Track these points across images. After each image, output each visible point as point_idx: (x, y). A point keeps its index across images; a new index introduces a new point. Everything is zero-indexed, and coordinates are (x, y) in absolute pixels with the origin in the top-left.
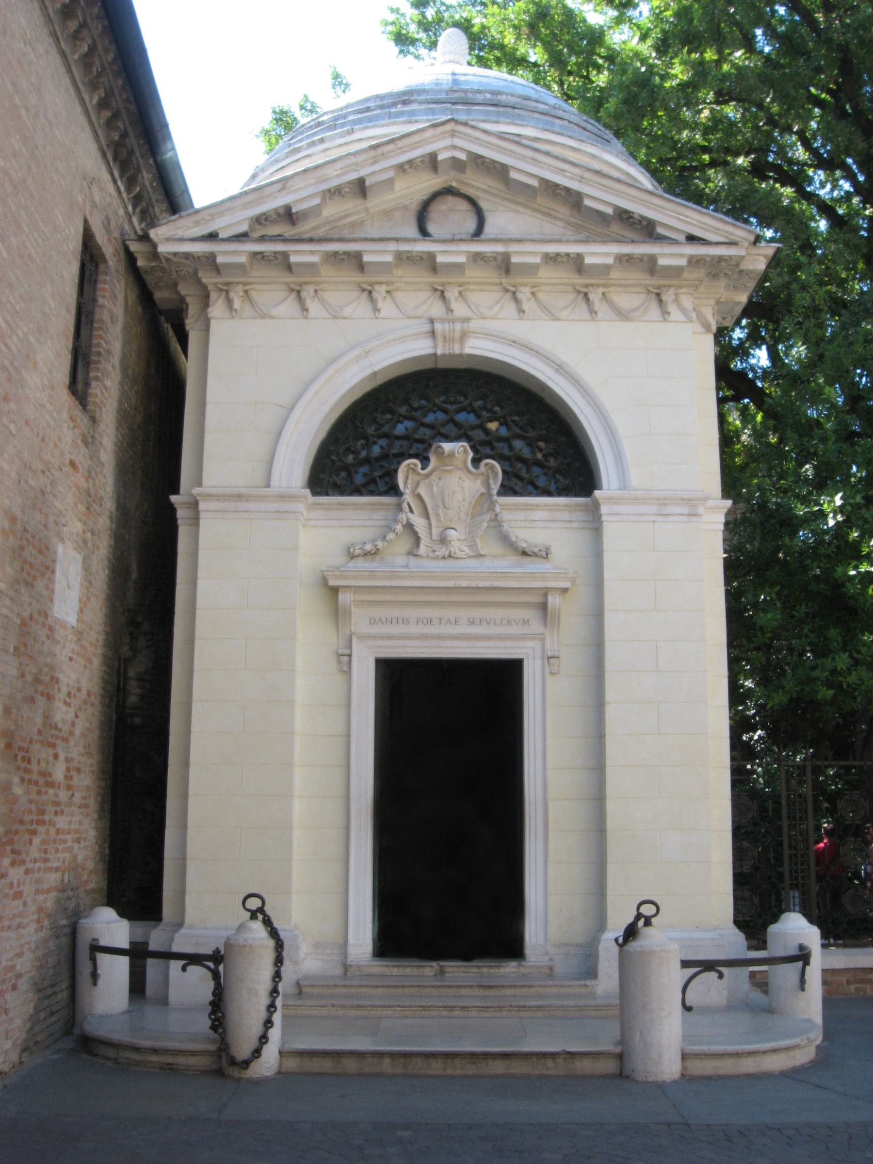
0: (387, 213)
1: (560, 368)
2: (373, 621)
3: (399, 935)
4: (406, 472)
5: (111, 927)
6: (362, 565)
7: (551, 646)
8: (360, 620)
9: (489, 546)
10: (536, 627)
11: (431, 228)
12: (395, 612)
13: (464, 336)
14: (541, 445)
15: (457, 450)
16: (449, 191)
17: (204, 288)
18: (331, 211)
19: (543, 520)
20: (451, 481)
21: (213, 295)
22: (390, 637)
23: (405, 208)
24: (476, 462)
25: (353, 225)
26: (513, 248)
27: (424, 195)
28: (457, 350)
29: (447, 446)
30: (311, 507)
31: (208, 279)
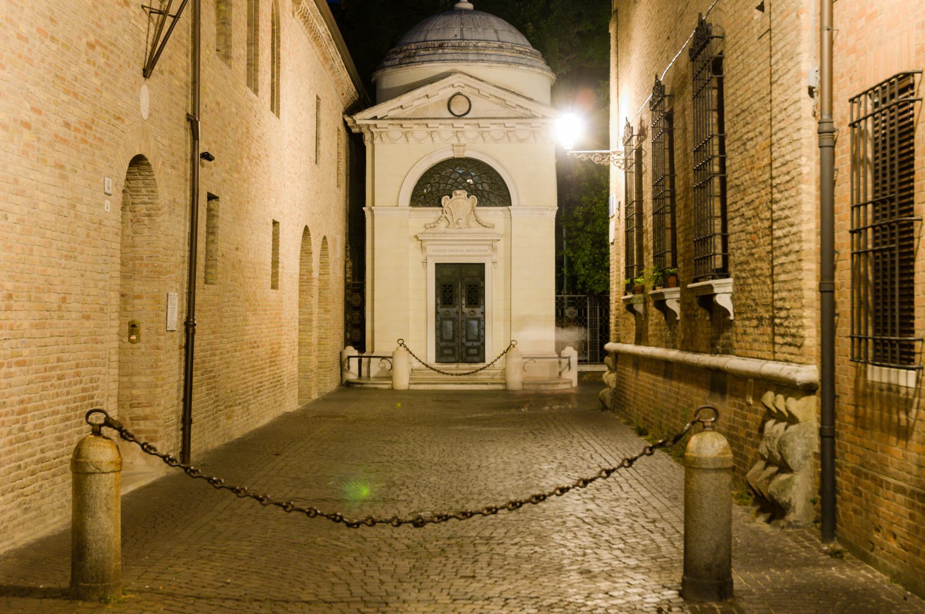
0: (437, 103)
1: (497, 162)
2: (434, 251)
3: (442, 355)
4: (445, 200)
5: (351, 351)
6: (429, 231)
7: (494, 258)
8: (430, 249)
9: (473, 223)
10: (490, 252)
11: (452, 109)
12: (441, 247)
13: (464, 151)
14: (490, 188)
15: (462, 193)
16: (459, 94)
17: (372, 133)
18: (415, 103)
19: (493, 214)
20: (460, 202)
21: (375, 135)
22: (440, 256)
23: (443, 101)
24: (468, 196)
25: (424, 108)
26: (480, 121)
27: (450, 96)
28: (462, 155)
29: (458, 192)
30: (411, 211)
31: (373, 130)
